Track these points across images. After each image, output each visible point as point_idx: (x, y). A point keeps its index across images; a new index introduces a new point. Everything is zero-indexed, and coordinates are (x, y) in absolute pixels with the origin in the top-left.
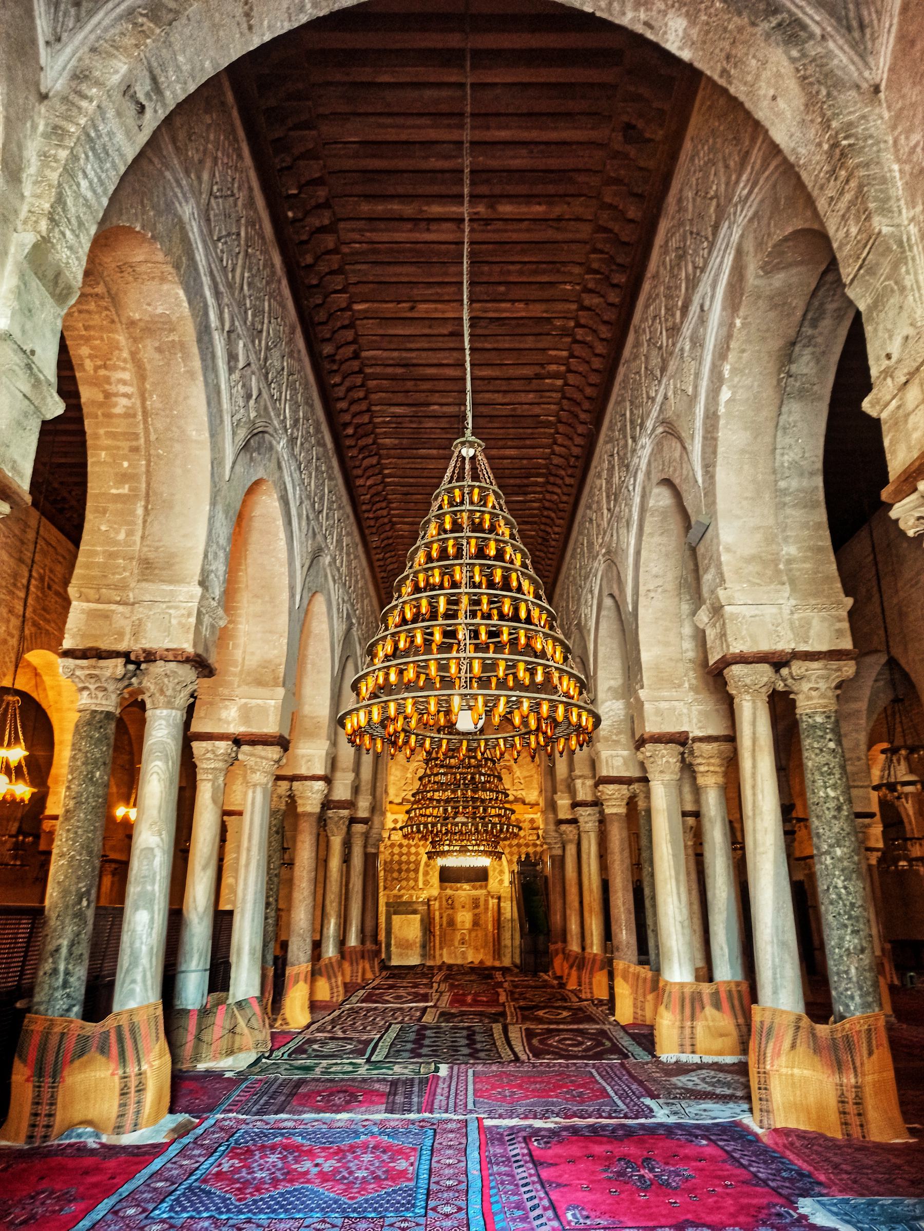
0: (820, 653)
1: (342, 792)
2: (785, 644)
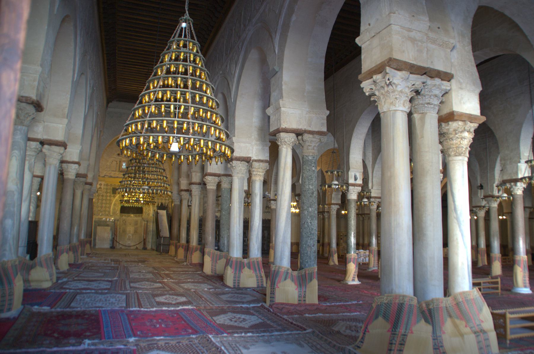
0: (314, 131)
1: (82, 171)
2: (302, 126)
